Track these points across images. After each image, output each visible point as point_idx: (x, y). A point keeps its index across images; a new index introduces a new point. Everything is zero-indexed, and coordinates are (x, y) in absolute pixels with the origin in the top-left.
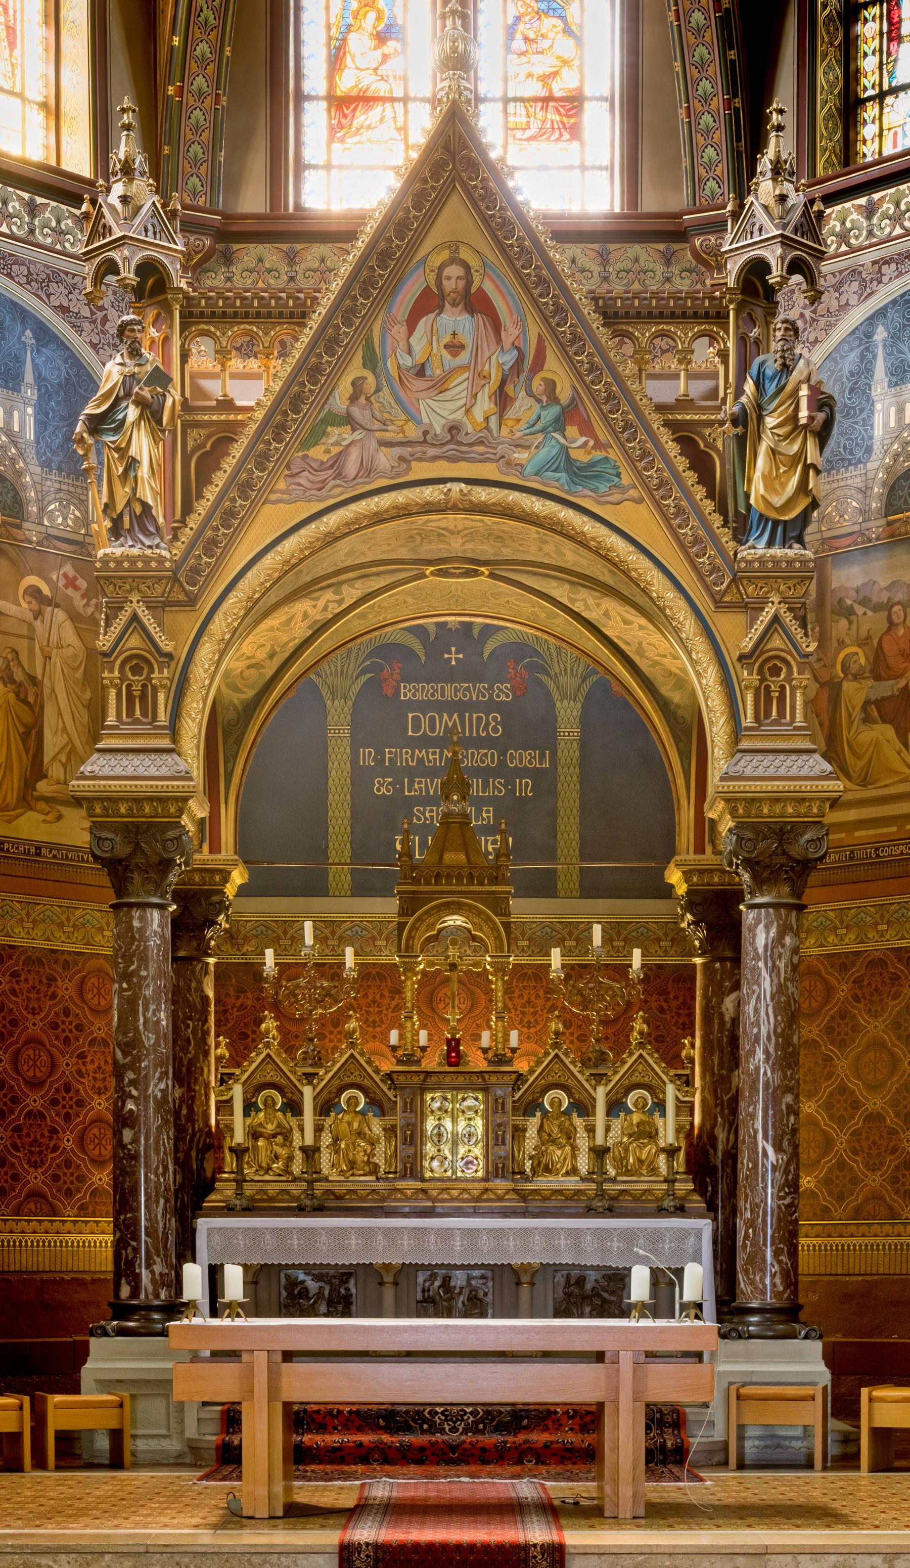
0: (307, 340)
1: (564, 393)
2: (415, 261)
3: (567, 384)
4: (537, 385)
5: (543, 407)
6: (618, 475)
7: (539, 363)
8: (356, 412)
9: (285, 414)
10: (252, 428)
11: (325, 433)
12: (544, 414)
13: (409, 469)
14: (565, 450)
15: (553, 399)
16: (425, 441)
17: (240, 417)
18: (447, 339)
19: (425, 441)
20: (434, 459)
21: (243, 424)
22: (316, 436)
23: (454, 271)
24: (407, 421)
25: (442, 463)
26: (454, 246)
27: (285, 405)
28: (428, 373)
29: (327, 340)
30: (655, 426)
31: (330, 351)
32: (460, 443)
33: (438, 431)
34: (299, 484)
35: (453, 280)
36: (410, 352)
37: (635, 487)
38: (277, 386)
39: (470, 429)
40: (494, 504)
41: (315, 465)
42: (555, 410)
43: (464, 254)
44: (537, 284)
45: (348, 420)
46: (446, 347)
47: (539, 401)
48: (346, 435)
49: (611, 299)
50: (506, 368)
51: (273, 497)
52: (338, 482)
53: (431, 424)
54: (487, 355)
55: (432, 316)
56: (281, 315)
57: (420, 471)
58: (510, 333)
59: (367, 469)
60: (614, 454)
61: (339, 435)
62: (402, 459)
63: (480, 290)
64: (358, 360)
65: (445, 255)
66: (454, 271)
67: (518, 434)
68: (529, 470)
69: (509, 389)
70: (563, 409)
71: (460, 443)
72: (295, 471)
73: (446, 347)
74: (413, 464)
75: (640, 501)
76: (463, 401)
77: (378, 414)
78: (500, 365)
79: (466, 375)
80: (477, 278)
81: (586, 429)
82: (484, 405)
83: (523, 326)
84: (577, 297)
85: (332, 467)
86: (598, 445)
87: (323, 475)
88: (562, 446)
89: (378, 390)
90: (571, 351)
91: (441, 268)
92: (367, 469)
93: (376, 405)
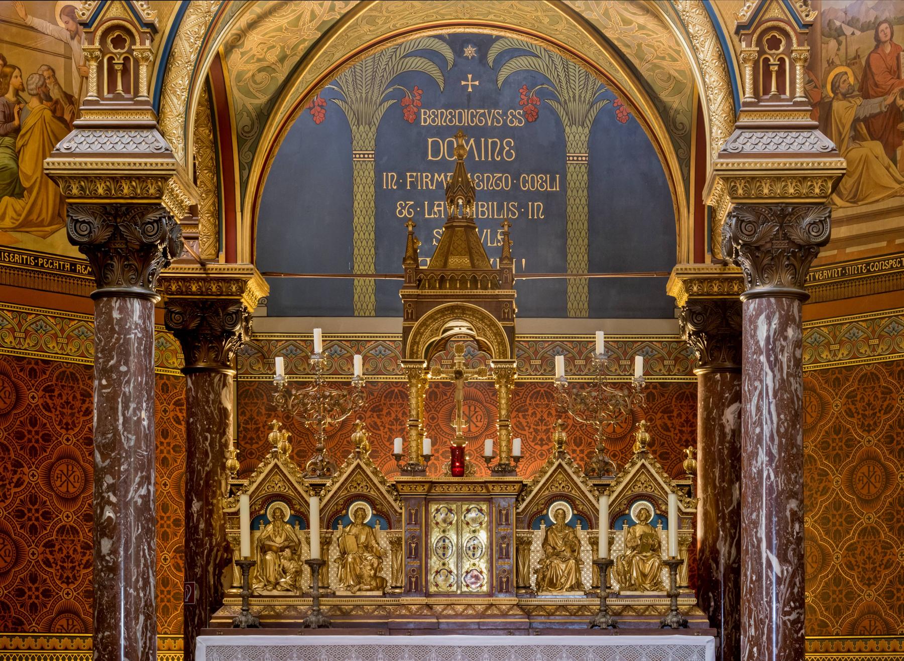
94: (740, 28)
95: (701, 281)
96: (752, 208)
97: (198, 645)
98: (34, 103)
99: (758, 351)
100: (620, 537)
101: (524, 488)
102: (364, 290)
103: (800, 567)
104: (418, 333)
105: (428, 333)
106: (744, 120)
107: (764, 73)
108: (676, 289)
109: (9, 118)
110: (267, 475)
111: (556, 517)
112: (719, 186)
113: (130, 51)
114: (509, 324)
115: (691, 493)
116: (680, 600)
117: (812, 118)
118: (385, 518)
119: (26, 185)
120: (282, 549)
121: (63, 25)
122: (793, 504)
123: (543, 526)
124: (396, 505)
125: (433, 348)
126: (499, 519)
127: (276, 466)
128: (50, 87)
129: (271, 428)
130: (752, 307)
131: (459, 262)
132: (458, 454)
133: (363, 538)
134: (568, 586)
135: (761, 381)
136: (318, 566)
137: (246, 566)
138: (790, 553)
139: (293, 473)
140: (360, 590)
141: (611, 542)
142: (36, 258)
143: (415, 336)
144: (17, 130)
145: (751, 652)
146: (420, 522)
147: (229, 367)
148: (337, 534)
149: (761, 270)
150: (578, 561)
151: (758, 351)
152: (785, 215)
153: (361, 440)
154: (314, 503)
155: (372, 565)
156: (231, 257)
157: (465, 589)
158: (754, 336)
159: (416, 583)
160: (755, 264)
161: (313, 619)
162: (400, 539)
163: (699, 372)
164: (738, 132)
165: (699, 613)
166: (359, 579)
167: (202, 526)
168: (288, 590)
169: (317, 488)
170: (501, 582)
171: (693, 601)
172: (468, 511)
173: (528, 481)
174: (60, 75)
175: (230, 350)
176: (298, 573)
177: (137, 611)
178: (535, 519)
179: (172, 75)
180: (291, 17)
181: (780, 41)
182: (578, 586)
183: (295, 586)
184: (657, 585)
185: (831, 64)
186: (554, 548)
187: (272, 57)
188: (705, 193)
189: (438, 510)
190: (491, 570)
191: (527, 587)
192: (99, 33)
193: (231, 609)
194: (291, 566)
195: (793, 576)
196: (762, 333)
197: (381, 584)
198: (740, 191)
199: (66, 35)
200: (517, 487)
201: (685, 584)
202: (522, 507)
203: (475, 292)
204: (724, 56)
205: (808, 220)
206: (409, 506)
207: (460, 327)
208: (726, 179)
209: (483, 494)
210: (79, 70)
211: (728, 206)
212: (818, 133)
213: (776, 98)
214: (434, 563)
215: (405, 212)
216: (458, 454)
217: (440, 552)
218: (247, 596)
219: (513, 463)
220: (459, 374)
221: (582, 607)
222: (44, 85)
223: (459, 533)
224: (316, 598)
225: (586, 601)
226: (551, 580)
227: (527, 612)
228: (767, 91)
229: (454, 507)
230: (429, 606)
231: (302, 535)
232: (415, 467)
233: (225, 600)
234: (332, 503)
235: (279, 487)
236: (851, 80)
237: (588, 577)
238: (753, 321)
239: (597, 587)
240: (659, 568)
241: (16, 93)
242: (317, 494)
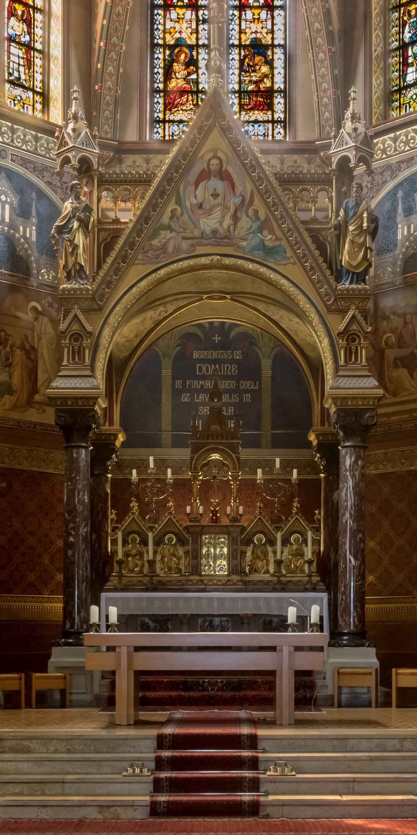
0: (151, 192)
2: (198, 157)
3: (263, 212)
4: (250, 212)
5: (253, 222)
6: (286, 252)
7: (251, 203)
8: (173, 225)
9: (142, 225)
10: (128, 231)
11: (159, 234)
12: (253, 225)
13: (195, 250)
14: (262, 241)
15: (258, 218)
16: (202, 237)
17: (122, 227)
18: (211, 192)
19: (202, 237)
20: (206, 245)
21: (123, 230)
22: (155, 234)
23: (215, 162)
24: (194, 228)
25: (209, 247)
26: (215, 150)
27: (142, 221)
28: (204, 207)
29: (160, 192)
30: (301, 230)
31: (161, 197)
32: (218, 238)
33: (208, 233)
34: (148, 257)
35: (215, 166)
36: (196, 198)
37: (293, 257)
38: (138, 213)
39: (221, 232)
40: (231, 265)
41: (154, 248)
42: (258, 223)
43: (220, 154)
44: (251, 167)
45: (169, 228)
46: (211, 195)
47: (251, 219)
48: (168, 234)
49: (282, 174)
50: (237, 204)
51: (137, 262)
52: (165, 255)
53: (205, 229)
54: (229, 198)
55: (206, 181)
56: (140, 181)
57: (200, 250)
58: (239, 189)
59: (177, 250)
60: (284, 243)
61: (165, 235)
62: (192, 245)
63: (226, 170)
64: (173, 200)
65: (211, 155)
66: (215, 162)
67: (243, 234)
68: (247, 250)
69: (239, 214)
70: (262, 222)
71: (218, 238)
72: (146, 250)
73: (211, 195)
74: (197, 247)
75: (295, 264)
76: (218, 219)
77: (182, 225)
78: (234, 203)
79: (219, 208)
80: (224, 164)
81: (272, 232)
82: (228, 221)
83: (244, 186)
84: (268, 173)
85: (162, 248)
86: (277, 239)
87: (158, 253)
88: (261, 239)
89: (182, 214)
90: (265, 197)
91: (210, 160)
93: (181, 221)
94: (339, 334)
95: (323, 435)
96: (344, 410)
97: (102, 597)
98: (18, 352)
99: (346, 470)
100: (286, 550)
101: (243, 529)
102: (166, 436)
103: (363, 562)
104: (197, 459)
105: (201, 459)
106: (340, 373)
107: (349, 353)
108: (312, 437)
109: (7, 359)
110: (129, 523)
111: (258, 541)
112: (330, 401)
113: (82, 344)
114: (237, 455)
115: (318, 530)
116: (313, 578)
117: (369, 372)
118: (182, 541)
119: (15, 389)
120: (136, 555)
121: (30, 315)
122: (360, 535)
123: (252, 545)
124: (187, 536)
125: (204, 465)
126: (232, 543)
127: (133, 518)
128: (25, 344)
129: (131, 502)
130: (343, 451)
131: (215, 427)
132: (215, 513)
133: (172, 551)
134: (263, 572)
135: (347, 483)
136: (151, 563)
137: (120, 563)
138: (359, 556)
139: (141, 522)
140: (170, 574)
141: (282, 552)
142: (19, 422)
143: (196, 461)
144: (11, 364)
145: (342, 598)
147: (109, 473)
148: (160, 549)
149: (347, 437)
150: (268, 561)
151: (346, 470)
152: (358, 413)
153: (171, 507)
154: (150, 535)
155: (176, 563)
156: (111, 424)
157: (217, 573)
158: (344, 464)
159: (196, 570)
160: (345, 433)
161: (151, 586)
162: (188, 551)
163: (322, 475)
164: (338, 378)
165: (321, 584)
166: (170, 569)
167: (97, 545)
168: (138, 574)
169: (151, 529)
170: (233, 570)
171: (319, 579)
172: (219, 538)
173: (245, 525)
174: (30, 338)
175: (109, 465)
176: (143, 566)
177: (83, 580)
178: (248, 542)
179: (98, 354)
180: (142, 319)
181: (356, 339)
182: (267, 572)
183: (141, 572)
184: (303, 571)
185: (385, 333)
186: (257, 555)
187: (132, 336)
188: (324, 402)
189: (205, 538)
190: (228, 565)
191: (245, 572)
192: (69, 336)
193: (114, 581)
194: (139, 563)
195: (360, 565)
196: (348, 462)
197: (179, 571)
198: (339, 403)
199: (32, 319)
200: (241, 528)
201: (315, 571)
202: (243, 537)
203: (223, 441)
204: (332, 344)
205: (367, 415)
206: (191, 537)
207: (215, 456)
208: (333, 398)
209: (226, 530)
210: (38, 336)
211: (333, 409)
212: (372, 378)
213: (354, 363)
214: (204, 561)
215: (186, 399)
216: (215, 513)
217: (206, 557)
218: (121, 576)
219: (239, 518)
220: (215, 477)
221: (269, 582)
222: (23, 343)
223: (215, 549)
224: (151, 577)
225: (271, 579)
226: (255, 569)
227: (245, 583)
228: (350, 360)
229: (213, 536)
230: (202, 581)
231: (144, 549)
232: (195, 518)
233: (111, 578)
234: (159, 535)
235: (135, 527)
236: (394, 340)
237: (272, 569)
238: (344, 457)
239: (276, 572)
240: (304, 564)
241: (11, 347)
242: (152, 531)
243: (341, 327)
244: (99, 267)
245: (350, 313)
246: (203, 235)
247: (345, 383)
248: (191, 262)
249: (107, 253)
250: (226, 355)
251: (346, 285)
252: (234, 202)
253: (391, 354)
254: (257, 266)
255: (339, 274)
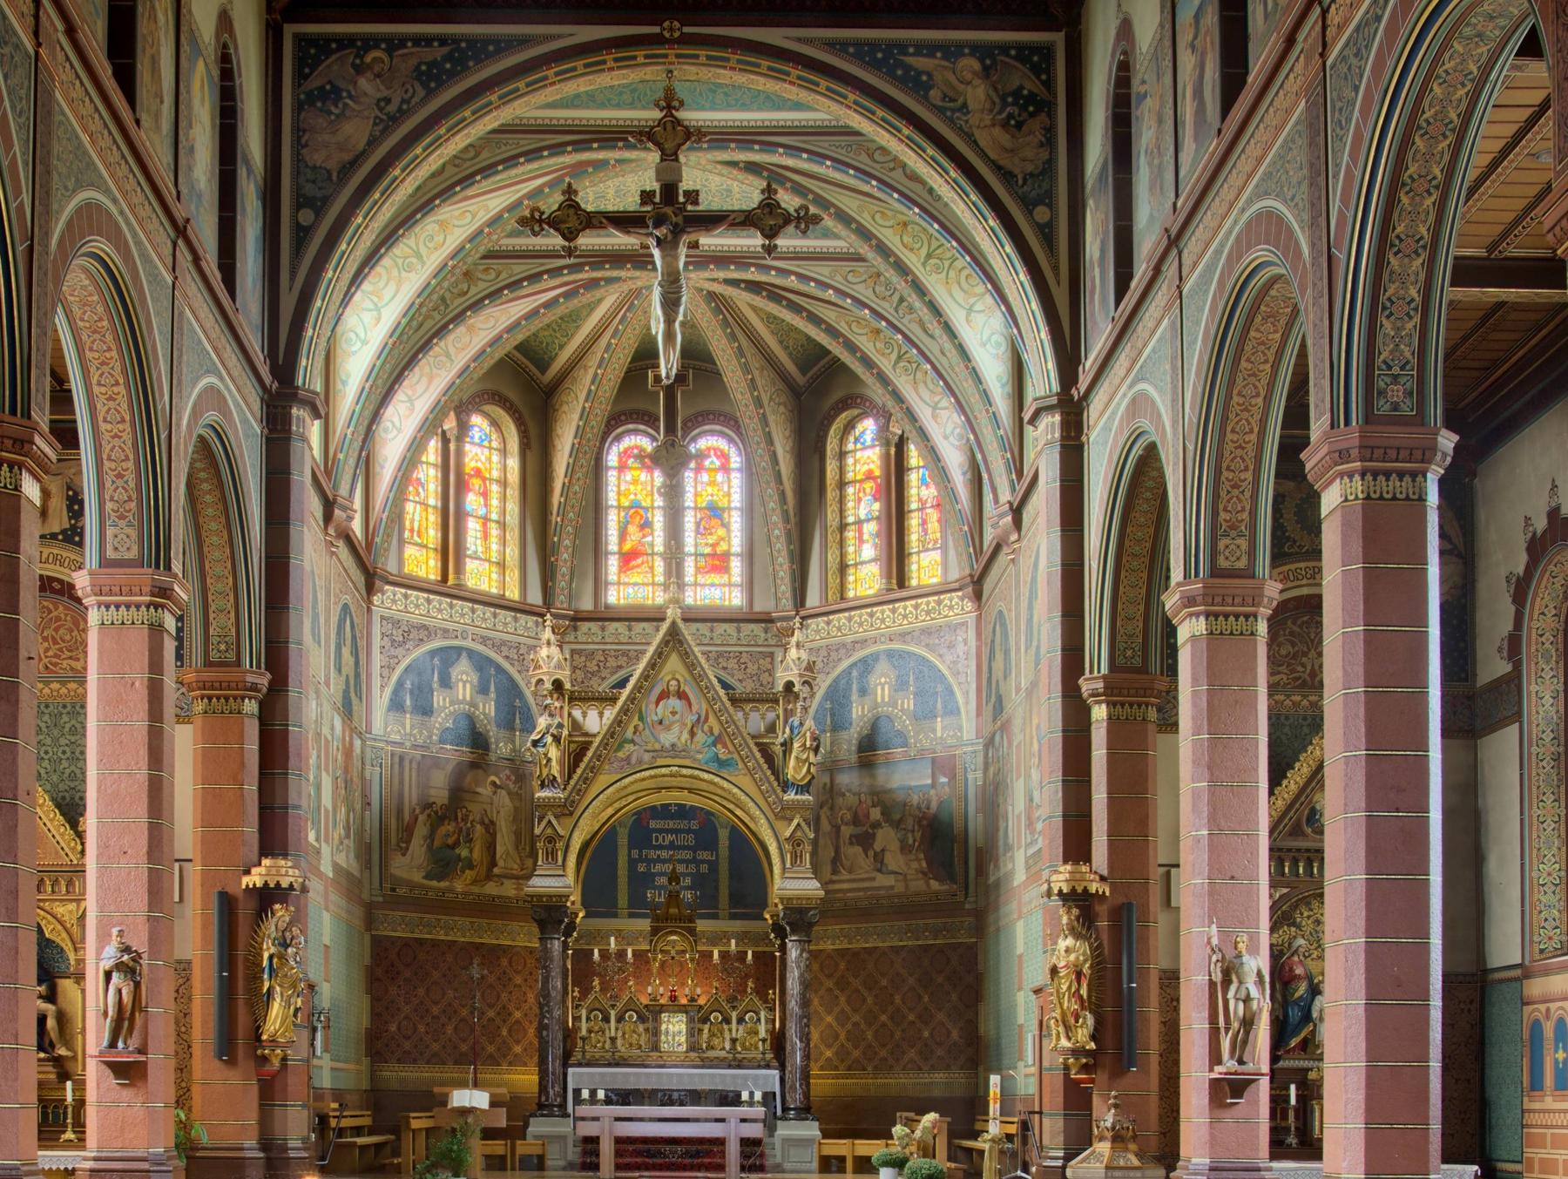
1: (716, 732)
4: (706, 728)
7: (706, 719)
48: (630, 747)
57: (660, 762)
58: (695, 707)
59: (640, 762)
60: (736, 756)
81: (725, 746)
82: (686, 736)
83: (700, 705)
92: (640, 762)
115: (772, 1009)
131: (673, 911)
146: (657, 1020)
243: (788, 834)
244: (570, 777)
245: (795, 822)
246: (662, 749)
247: (792, 883)
248: (652, 772)
249: (576, 765)
250: (683, 824)
251: (791, 796)
252: (690, 719)
253: (846, 831)
254: (712, 777)
255: (786, 786)
